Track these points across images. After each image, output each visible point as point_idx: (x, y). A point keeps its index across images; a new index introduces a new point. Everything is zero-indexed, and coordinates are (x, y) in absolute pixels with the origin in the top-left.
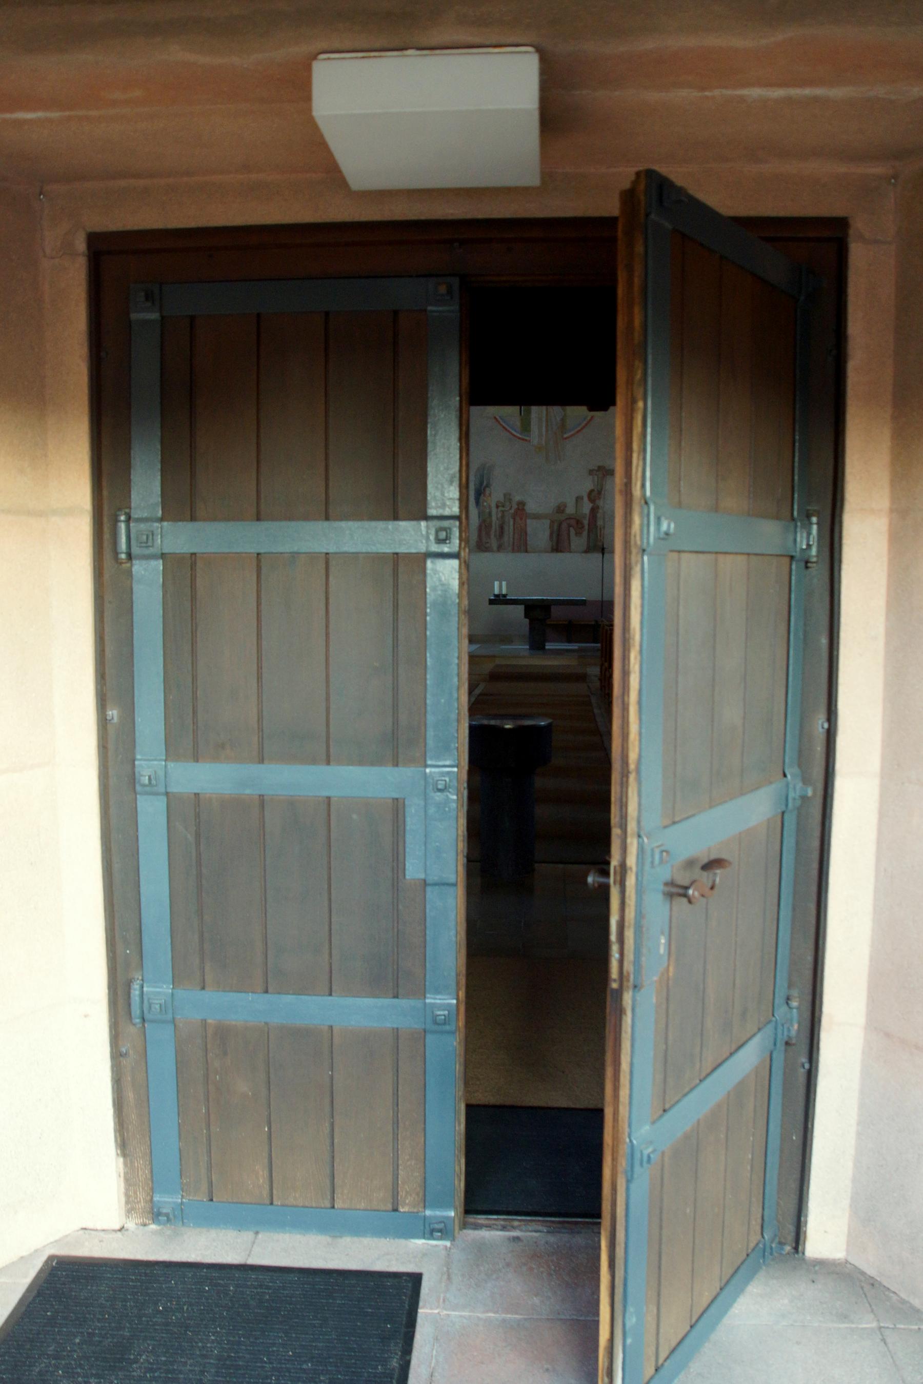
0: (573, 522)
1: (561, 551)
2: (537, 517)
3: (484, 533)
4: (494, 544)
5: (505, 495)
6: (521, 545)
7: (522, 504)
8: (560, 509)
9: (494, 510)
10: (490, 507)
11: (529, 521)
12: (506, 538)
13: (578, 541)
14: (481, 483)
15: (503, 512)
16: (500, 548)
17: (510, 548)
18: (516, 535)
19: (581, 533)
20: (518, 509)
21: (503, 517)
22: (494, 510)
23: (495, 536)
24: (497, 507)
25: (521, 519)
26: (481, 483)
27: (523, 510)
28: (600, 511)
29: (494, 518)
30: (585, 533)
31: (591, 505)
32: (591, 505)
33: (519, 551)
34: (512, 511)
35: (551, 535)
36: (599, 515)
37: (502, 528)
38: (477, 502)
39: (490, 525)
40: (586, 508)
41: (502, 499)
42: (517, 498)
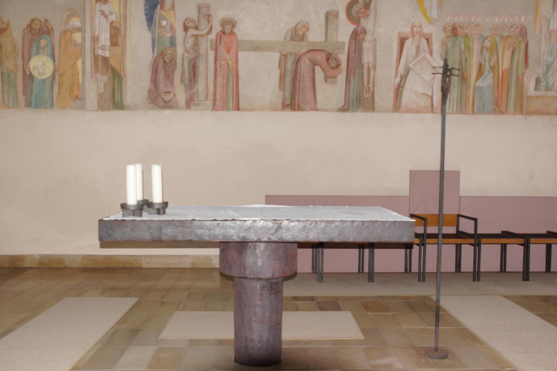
0: (321, 57)
1: (300, 109)
2: (256, 47)
3: (161, 76)
4: (181, 95)
5: (199, 8)
6: (229, 98)
7: (229, 26)
8: (298, 34)
9: (180, 34)
10: (172, 28)
11: (242, 55)
12: (201, 85)
13: (331, 92)
15: (196, 37)
16: (190, 103)
17: (209, 103)
18: (219, 79)
19: (335, 77)
20: (224, 33)
21: (196, 45)
22: (180, 34)
23: (182, 81)
24: (186, 29)
25: (228, 51)
27: (232, 33)
28: (368, 37)
29: (180, 50)
30: (342, 78)
31: (352, 27)
32: (352, 27)
33: (225, 108)
34: (213, 36)
35: (282, 78)
36: (366, 45)
37: (194, 68)
38: (150, 19)
39: (173, 59)
40: (344, 31)
41: (194, 15)
42: (220, 14)
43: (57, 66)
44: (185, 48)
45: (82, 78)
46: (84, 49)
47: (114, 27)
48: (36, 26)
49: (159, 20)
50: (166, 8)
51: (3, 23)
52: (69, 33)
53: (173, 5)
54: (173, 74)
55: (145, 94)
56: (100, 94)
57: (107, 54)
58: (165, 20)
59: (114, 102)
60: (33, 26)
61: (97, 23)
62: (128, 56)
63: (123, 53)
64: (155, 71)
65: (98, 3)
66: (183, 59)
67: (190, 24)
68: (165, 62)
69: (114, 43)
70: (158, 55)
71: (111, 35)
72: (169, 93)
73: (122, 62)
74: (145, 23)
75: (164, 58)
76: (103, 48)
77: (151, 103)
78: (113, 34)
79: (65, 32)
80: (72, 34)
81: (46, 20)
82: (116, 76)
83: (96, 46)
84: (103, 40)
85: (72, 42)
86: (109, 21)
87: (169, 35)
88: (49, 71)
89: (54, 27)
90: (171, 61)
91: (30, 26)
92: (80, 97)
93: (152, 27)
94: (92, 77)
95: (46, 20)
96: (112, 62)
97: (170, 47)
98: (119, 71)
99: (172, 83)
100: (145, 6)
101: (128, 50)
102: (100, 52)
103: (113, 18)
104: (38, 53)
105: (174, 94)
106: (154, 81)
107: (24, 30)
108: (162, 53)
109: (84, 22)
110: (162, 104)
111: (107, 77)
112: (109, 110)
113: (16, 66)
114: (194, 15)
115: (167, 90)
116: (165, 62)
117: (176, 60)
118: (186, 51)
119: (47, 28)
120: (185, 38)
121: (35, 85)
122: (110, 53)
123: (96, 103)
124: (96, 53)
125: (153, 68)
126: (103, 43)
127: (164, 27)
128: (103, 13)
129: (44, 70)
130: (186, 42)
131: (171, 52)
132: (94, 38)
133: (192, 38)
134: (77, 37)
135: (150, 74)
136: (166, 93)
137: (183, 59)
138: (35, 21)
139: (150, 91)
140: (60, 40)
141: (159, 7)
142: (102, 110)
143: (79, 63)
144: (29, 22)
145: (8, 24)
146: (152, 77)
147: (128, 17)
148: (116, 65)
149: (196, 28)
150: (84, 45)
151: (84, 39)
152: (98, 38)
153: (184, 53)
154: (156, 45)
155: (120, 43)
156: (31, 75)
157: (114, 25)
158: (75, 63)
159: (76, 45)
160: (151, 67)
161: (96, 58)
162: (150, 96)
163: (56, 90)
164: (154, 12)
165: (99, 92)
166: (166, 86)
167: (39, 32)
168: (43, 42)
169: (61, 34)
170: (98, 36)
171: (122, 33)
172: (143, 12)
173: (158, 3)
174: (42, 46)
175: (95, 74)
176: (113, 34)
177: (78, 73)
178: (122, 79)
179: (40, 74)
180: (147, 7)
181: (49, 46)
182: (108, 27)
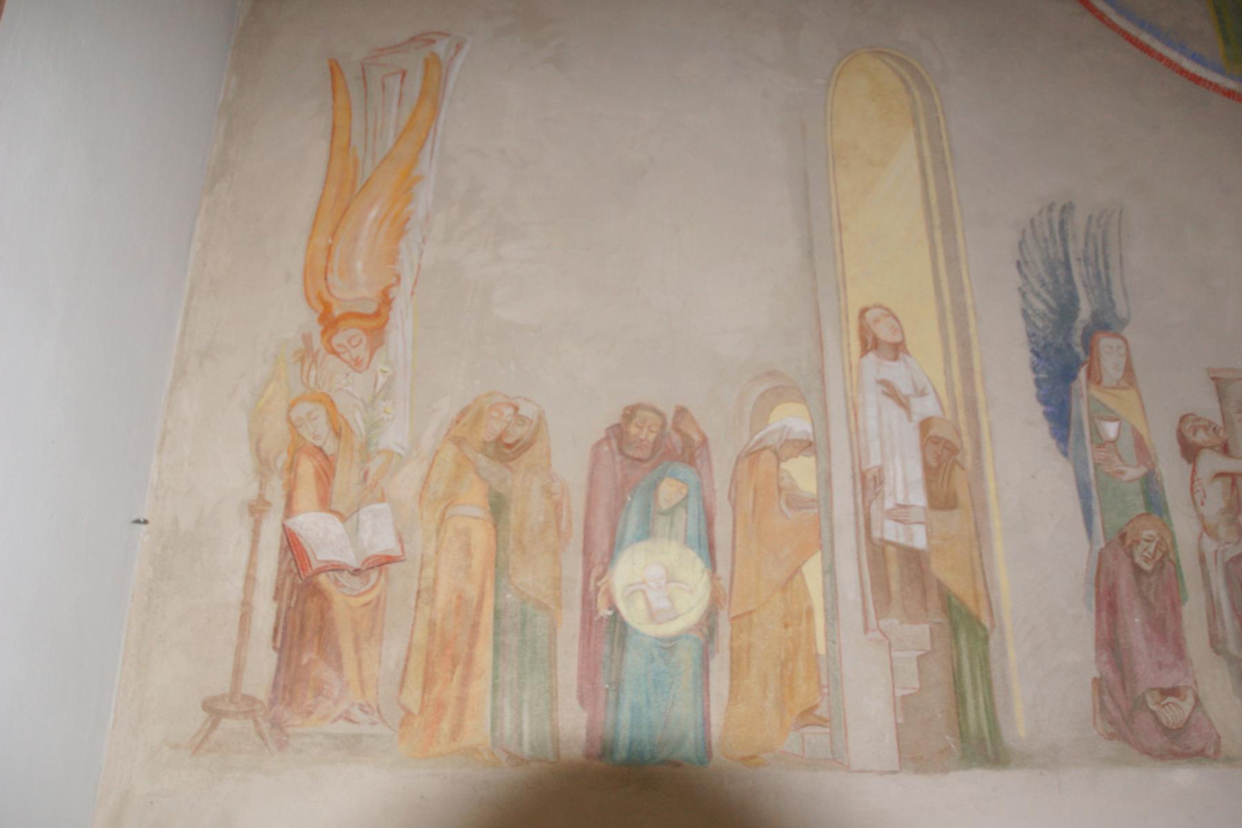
3: (1135, 622)
9: (1172, 472)
10: (1141, 446)
14: (1066, 311)
22: (1172, 472)
23: (1215, 643)
24: (1190, 452)
26: (1066, 311)
29: (1185, 528)
38: (1060, 418)
39: (1166, 560)
43: (725, 583)
44: (1201, 517)
45: (826, 633)
46: (830, 519)
47: (936, 441)
48: (643, 433)
49: (1091, 419)
50: (1106, 381)
51: (519, 419)
52: (767, 455)
53: (1129, 370)
54: (1177, 616)
55: (1084, 699)
56: (903, 696)
57: (920, 540)
58: (1112, 420)
59: (963, 736)
60: (633, 430)
61: (872, 424)
62: (999, 547)
63: (978, 536)
64: (1107, 604)
65: (871, 355)
66: (1202, 560)
67: (1201, 437)
68: (1137, 570)
69: (941, 498)
70: (1107, 545)
71: (926, 467)
72: (1173, 692)
73: (980, 570)
74: (1043, 429)
75: (1131, 556)
76: (901, 513)
77: (1111, 737)
78: (934, 464)
79: (752, 455)
80: (779, 460)
81: (681, 412)
82: (963, 626)
83: (874, 507)
84: (900, 487)
85: (780, 489)
86: (917, 419)
87: (1134, 472)
88: (690, 606)
89: (709, 435)
90: (1160, 565)
91: (618, 434)
92: (822, 711)
93: (1072, 440)
94: (866, 629)
95: (681, 412)
96: (940, 569)
97: (1148, 514)
98: (970, 603)
99: (1180, 651)
100: (1035, 369)
101: (996, 523)
102: (891, 531)
103: (927, 407)
104: (647, 533)
105: (1197, 699)
106: (1111, 643)
107: (598, 445)
108: (1123, 537)
109: (822, 416)
110: (1158, 741)
111: (926, 627)
112: (946, 770)
113: (557, 582)
114: (1209, 408)
115: (1167, 682)
116: (1137, 570)
117: (1176, 565)
118: (1207, 529)
119: (685, 437)
120: (1193, 482)
121: (634, 661)
122: (929, 536)
123: (890, 739)
124: (876, 534)
125: (1098, 595)
126: (900, 499)
127: (1113, 442)
128: (890, 390)
129: (670, 598)
130: (1198, 497)
131: (1152, 532)
132: (863, 477)
133: (1219, 484)
134: (801, 473)
135: (1093, 616)
136: (1165, 693)
137: (1202, 560)
138: (641, 414)
139: (1099, 685)
140: (734, 482)
141: (1082, 374)
142: (917, 771)
143: (813, 571)
144: (616, 420)
145: (539, 426)
146: (1098, 626)
147: (981, 405)
148: (958, 584)
149: (1225, 450)
150: (829, 501)
151: (826, 480)
152: (879, 480)
153: (1200, 538)
154: (1096, 507)
155: (963, 498)
156: (617, 623)
157: (932, 432)
158: (797, 570)
159: (796, 502)
160: (1093, 591)
161: (877, 552)
162: (1102, 704)
163: (719, 682)
164: (1068, 392)
165: (899, 693)
166: (1160, 665)
167: (654, 451)
168: (669, 491)
169: (738, 460)
170: (880, 469)
171: (968, 461)
172: (1032, 389)
173: (1078, 364)
174: (664, 506)
175: (877, 619)
176: (934, 464)
177: (810, 613)
178: (986, 639)
179: (653, 617)
180: (1042, 376)
181: (694, 506)
182: (914, 437)
